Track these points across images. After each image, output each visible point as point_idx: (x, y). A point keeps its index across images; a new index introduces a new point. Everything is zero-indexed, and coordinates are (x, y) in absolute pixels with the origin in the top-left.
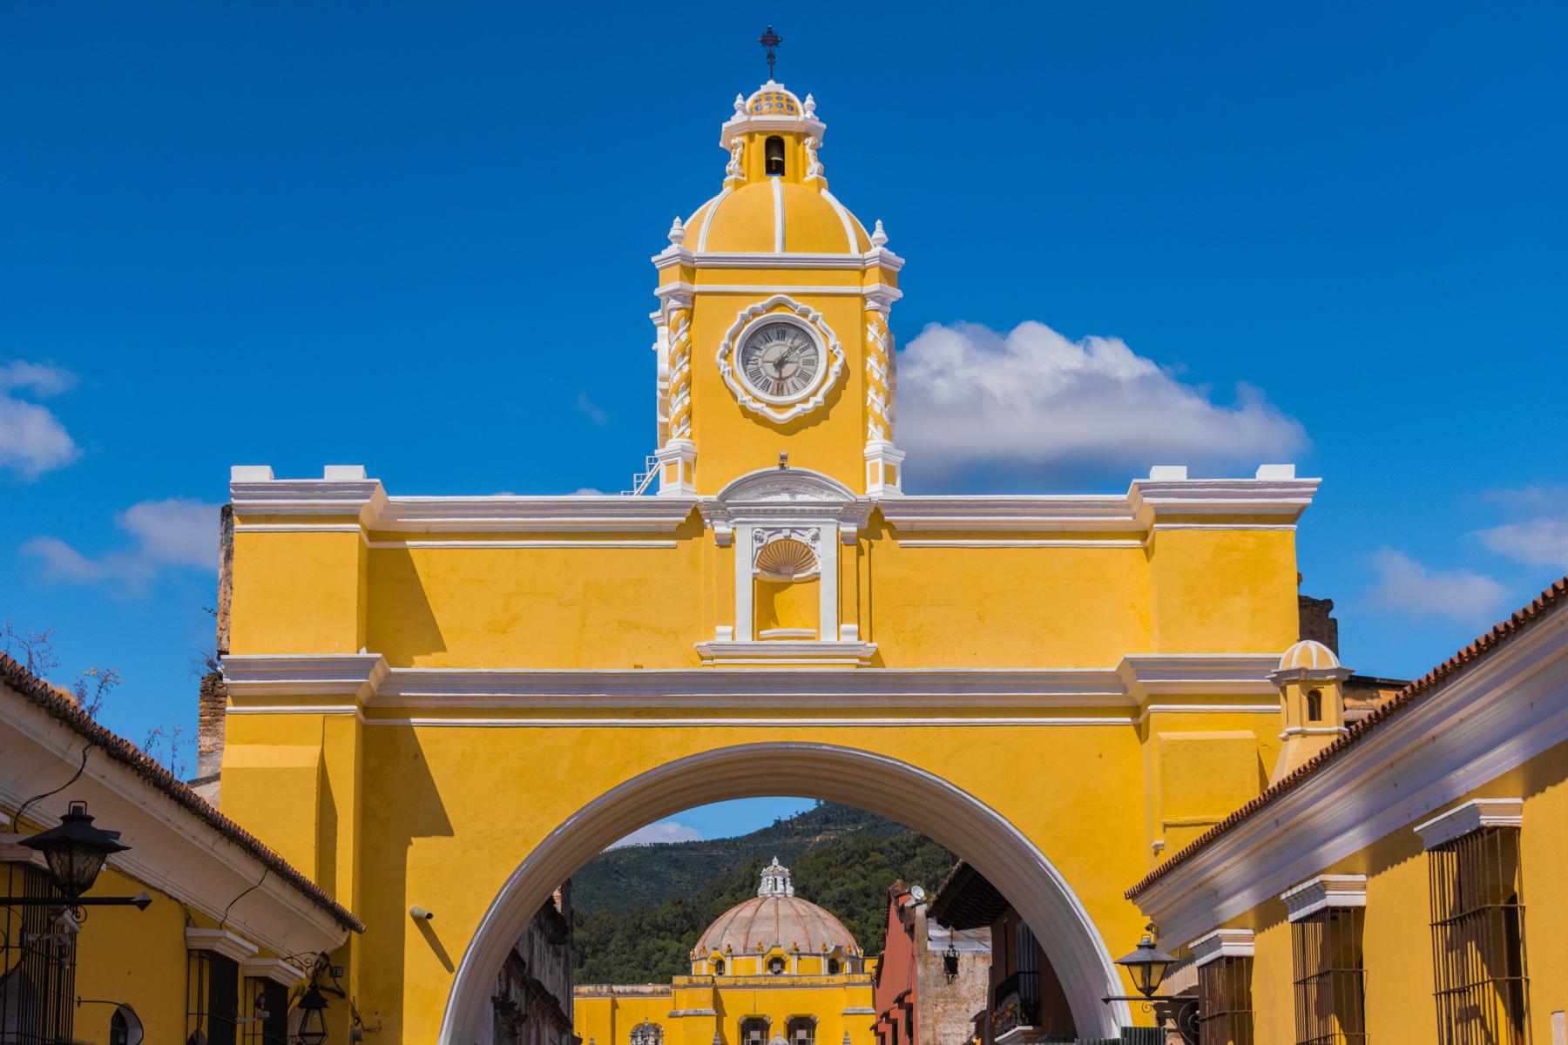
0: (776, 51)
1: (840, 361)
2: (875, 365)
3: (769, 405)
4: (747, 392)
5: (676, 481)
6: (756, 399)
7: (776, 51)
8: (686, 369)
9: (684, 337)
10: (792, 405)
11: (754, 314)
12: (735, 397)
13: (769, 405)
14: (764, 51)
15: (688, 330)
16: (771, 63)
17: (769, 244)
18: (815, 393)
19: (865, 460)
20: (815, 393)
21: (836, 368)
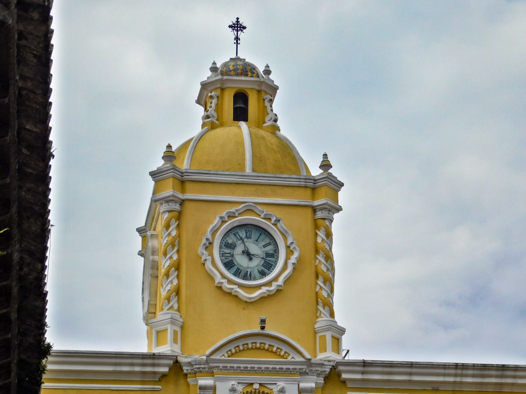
0: (241, 35)
1: (296, 255)
2: (323, 260)
3: (240, 286)
4: (223, 276)
5: (166, 344)
6: (230, 282)
7: (241, 35)
8: (175, 257)
9: (174, 233)
10: (259, 287)
11: (231, 216)
12: (211, 278)
13: (240, 286)
14: (232, 34)
15: (178, 226)
16: (237, 43)
17: (242, 167)
18: (276, 279)
19: (315, 333)
20: (276, 279)
21: (293, 259)
